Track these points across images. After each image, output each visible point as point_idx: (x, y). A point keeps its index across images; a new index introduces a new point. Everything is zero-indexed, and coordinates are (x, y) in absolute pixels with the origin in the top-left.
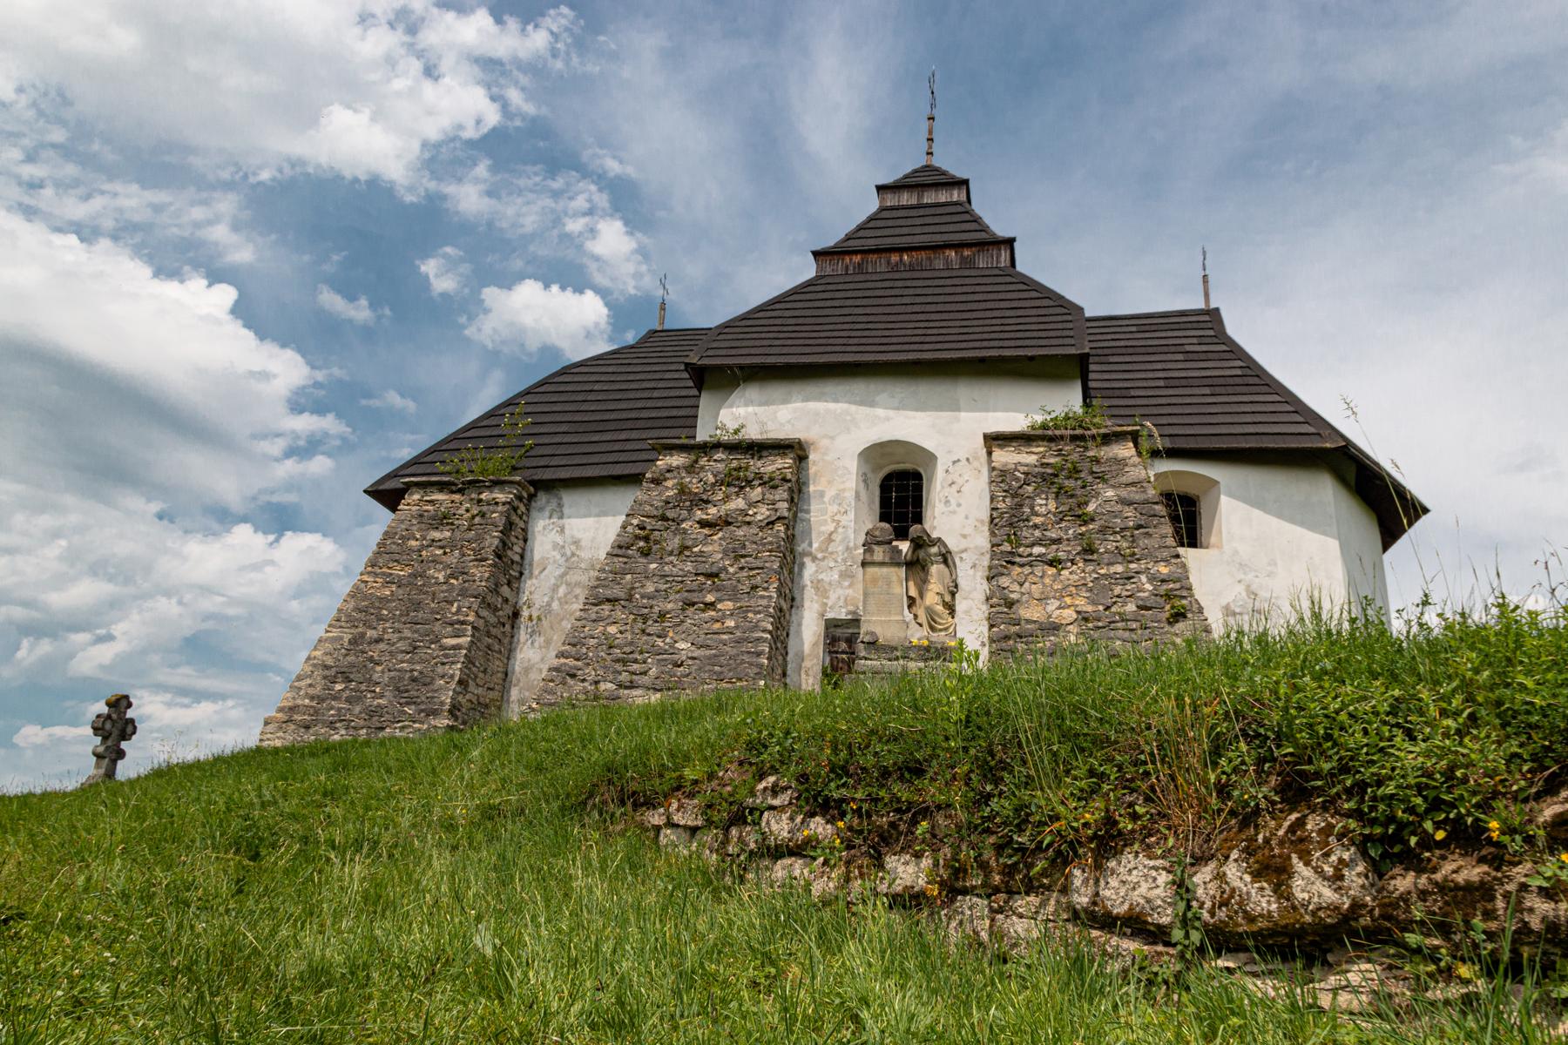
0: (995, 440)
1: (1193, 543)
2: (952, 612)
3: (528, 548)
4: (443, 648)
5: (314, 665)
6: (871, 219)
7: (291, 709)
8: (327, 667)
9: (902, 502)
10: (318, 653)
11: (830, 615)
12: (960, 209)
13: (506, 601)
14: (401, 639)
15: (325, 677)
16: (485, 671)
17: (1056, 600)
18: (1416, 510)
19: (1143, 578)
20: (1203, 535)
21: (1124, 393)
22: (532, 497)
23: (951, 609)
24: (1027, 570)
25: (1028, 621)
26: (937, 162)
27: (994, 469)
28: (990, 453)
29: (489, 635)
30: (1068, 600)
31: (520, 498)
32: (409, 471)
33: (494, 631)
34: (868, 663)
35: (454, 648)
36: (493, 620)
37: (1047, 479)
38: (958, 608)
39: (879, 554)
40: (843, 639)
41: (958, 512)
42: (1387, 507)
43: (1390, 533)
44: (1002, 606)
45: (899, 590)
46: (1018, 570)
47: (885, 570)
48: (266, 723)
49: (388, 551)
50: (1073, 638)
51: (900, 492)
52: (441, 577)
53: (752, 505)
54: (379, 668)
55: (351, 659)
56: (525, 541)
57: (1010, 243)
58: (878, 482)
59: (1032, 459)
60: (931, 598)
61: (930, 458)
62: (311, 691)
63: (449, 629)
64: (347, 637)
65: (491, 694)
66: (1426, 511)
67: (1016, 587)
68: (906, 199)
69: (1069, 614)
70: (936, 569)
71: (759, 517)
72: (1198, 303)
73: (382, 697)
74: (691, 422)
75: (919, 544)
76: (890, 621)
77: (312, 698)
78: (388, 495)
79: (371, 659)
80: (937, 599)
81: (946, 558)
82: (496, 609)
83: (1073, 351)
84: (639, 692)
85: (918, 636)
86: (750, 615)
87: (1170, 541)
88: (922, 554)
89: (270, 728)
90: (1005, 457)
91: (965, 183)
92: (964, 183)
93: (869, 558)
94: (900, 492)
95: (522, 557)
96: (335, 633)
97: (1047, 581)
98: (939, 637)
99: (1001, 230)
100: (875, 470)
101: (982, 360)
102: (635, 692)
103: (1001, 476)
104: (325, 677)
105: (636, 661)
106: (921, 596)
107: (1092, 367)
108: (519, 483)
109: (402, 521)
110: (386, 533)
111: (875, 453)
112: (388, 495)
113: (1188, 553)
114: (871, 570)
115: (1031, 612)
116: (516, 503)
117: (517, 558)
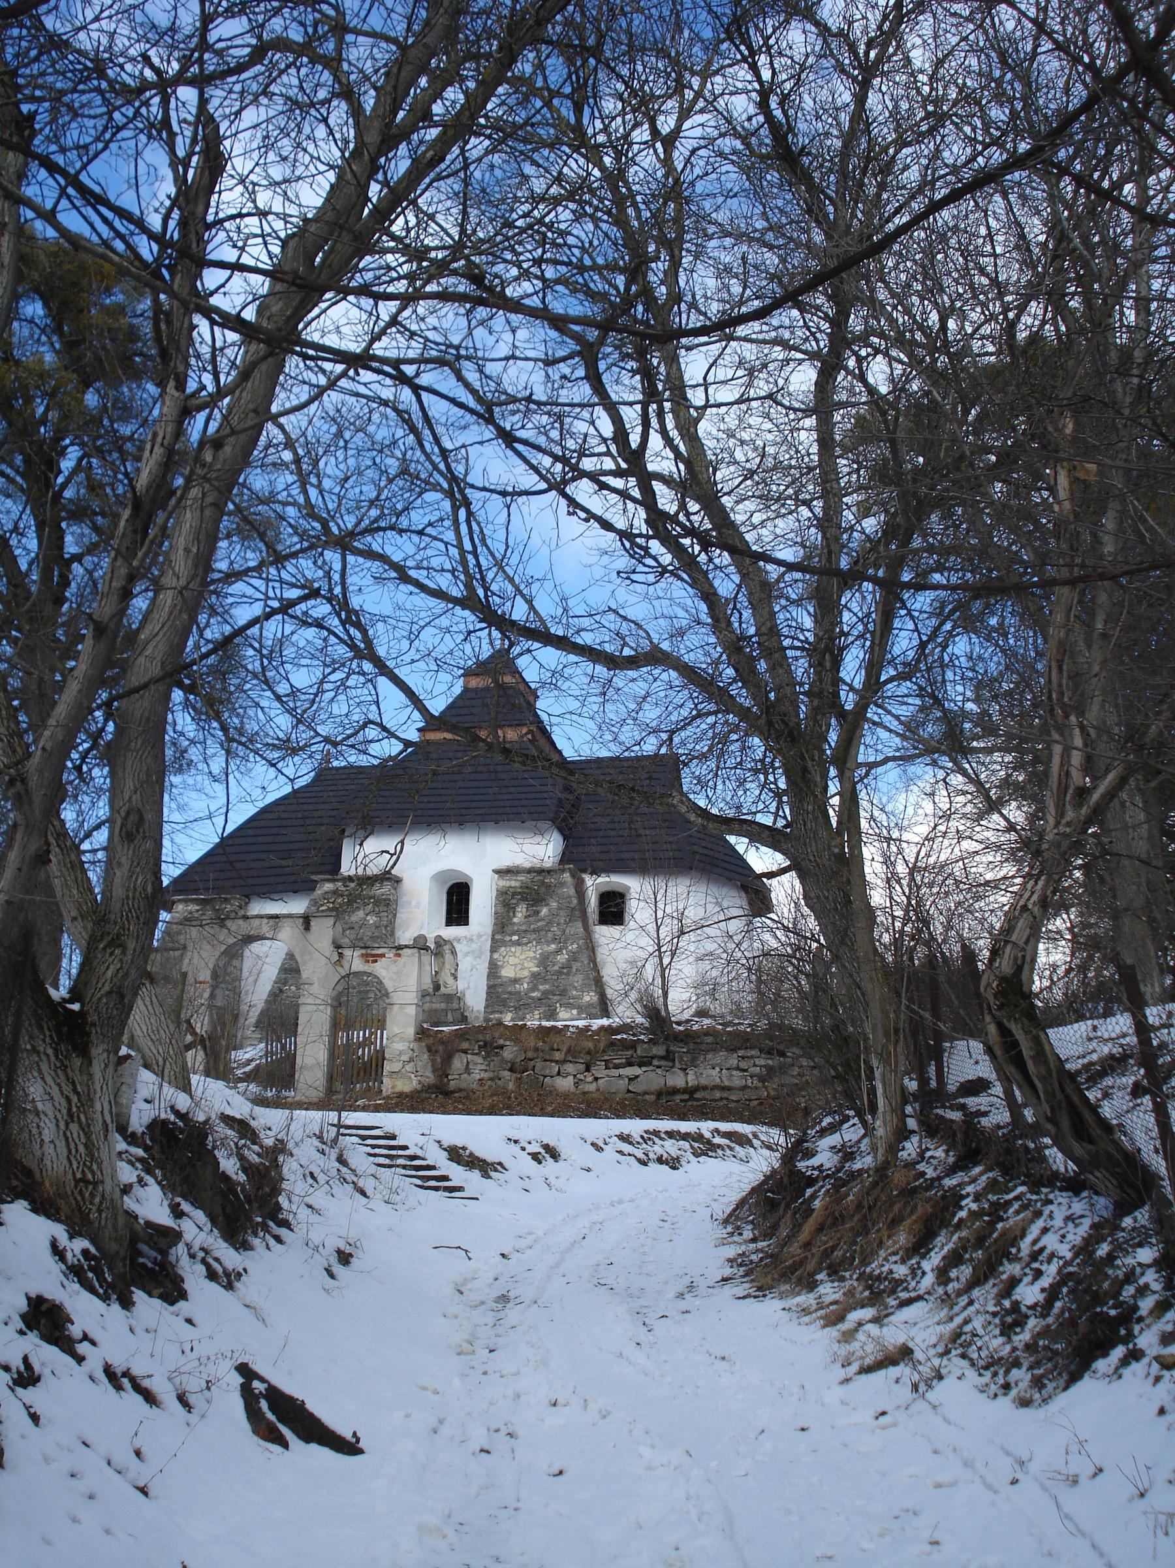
9: (459, 902)
44: (494, 969)
69: (526, 973)
70: (448, 957)
111: (439, 877)
115: (507, 972)
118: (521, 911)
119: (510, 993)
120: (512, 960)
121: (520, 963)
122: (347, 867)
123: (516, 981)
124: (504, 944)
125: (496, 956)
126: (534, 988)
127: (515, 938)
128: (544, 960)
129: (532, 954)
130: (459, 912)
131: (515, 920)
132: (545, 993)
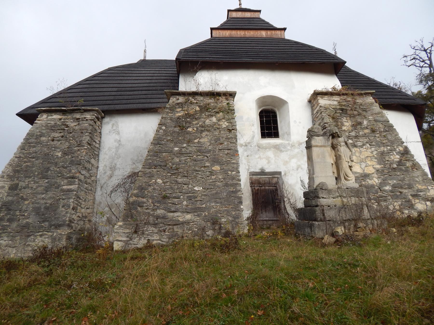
4: (63, 191)
9: (268, 122)
11: (252, 170)
13: (93, 165)
14: (39, 186)
16: (85, 201)
22: (103, 118)
31: (98, 118)
33: (89, 181)
35: (70, 190)
36: (87, 175)
47: (322, 149)
49: (29, 141)
50: (376, 180)
52: (59, 154)
53: (219, 120)
54: (26, 202)
55: (10, 198)
56: (100, 138)
59: (335, 103)
63: (66, 181)
64: (7, 188)
65: (88, 211)
71: (224, 126)
73: (28, 218)
78: (29, 116)
79: (22, 198)
82: (89, 170)
86: (230, 172)
90: (323, 102)
95: (100, 144)
100: (259, 107)
102: (176, 214)
105: (175, 198)
108: (97, 111)
109: (37, 128)
110: (28, 134)
116: (96, 120)
117: (97, 146)
129: (368, 153)
130: (269, 128)
132: (394, 186)
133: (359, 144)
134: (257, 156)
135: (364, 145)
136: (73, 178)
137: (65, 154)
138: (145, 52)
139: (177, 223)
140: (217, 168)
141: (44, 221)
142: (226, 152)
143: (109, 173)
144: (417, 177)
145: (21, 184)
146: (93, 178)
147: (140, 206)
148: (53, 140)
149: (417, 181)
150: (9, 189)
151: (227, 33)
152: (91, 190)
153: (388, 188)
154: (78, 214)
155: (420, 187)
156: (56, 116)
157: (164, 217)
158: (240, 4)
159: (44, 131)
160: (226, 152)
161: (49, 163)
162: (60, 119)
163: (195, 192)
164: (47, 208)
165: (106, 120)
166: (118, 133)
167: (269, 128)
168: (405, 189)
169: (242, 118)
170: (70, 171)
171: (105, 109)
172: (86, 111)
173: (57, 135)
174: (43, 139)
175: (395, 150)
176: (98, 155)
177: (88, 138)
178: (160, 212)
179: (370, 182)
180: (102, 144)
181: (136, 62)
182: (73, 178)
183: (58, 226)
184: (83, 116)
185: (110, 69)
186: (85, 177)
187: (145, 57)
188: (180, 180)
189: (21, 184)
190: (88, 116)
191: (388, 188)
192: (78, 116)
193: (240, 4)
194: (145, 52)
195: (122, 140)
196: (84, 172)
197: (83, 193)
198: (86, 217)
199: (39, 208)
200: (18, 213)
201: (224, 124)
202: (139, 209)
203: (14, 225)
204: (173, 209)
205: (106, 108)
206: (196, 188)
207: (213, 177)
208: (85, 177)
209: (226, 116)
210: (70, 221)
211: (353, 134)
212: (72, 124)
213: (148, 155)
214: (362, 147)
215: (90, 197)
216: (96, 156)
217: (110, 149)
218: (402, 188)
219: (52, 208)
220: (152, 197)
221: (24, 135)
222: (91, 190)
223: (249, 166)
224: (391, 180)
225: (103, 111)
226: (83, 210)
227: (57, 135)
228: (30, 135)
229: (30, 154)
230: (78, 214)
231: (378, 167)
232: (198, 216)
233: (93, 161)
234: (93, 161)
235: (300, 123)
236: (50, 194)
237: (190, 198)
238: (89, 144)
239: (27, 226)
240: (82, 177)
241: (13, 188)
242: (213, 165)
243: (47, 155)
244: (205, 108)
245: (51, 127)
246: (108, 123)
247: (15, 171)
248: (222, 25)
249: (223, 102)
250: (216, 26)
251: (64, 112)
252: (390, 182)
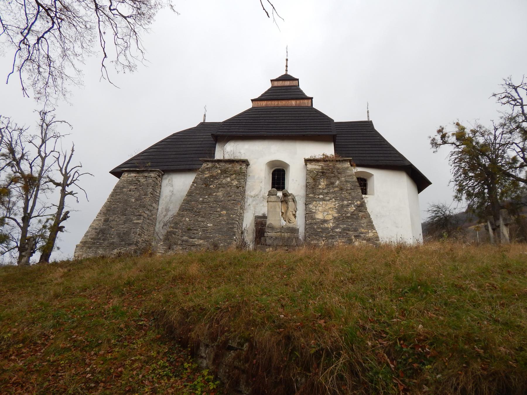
0: (307, 161)
1: (366, 194)
2: (295, 217)
3: (162, 191)
4: (134, 223)
5: (93, 229)
6: (269, 90)
7: (85, 242)
8: (96, 229)
10: (94, 225)
11: (257, 215)
12: (296, 88)
13: (154, 208)
15: (96, 232)
16: (147, 231)
17: (326, 211)
18: (429, 183)
19: (353, 206)
20: (368, 190)
21: (346, 146)
22: (163, 175)
23: (295, 216)
24: (318, 203)
25: (318, 219)
26: (289, 73)
27: (307, 170)
28: (306, 165)
29: (148, 219)
30: (330, 212)
31: (159, 176)
32: (125, 166)
34: (269, 234)
36: (150, 214)
37: (323, 173)
38: (297, 215)
39: (273, 198)
40: (261, 224)
41: (295, 183)
42: (421, 182)
43: (420, 190)
45: (279, 210)
46: (315, 202)
47: (274, 203)
48: (77, 247)
50: (331, 224)
51: (278, 175)
52: (133, 200)
53: (232, 180)
54: (113, 230)
55: (104, 227)
57: (312, 98)
58: (271, 172)
60: (290, 214)
61: (287, 165)
62: (92, 237)
64: (103, 220)
66: (429, 183)
67: (314, 208)
68: (280, 83)
69: (330, 217)
70: (291, 203)
71: (234, 184)
72: (367, 120)
74: (212, 153)
75: (285, 195)
76: (276, 220)
77: (92, 239)
78: (117, 173)
79: (111, 227)
80: (291, 213)
81: (294, 201)
82: (151, 211)
83: (330, 133)
84: (196, 240)
85: (284, 223)
87: (360, 194)
88: (286, 199)
89: (78, 248)
90: (310, 166)
91: (298, 80)
92: (298, 80)
93: (269, 200)
94: (278, 175)
95: (160, 193)
96: (99, 218)
97: (324, 206)
98: (291, 225)
99: (308, 95)
100: (271, 168)
101: (304, 136)
102: (194, 240)
103: (309, 172)
104: (96, 232)
105: (195, 230)
106: (286, 212)
107: (337, 138)
110: (116, 186)
112: (117, 173)
113: (364, 196)
114: (270, 203)
115: (320, 216)
116: (158, 177)
117: (158, 194)
118: (323, 183)
119: (322, 228)
120: (320, 209)
121: (326, 211)
122: (218, 155)
123: (325, 221)
124: (313, 199)
125: (311, 206)
126: (337, 227)
127: (321, 196)
128: (341, 209)
129: (332, 206)
130: (278, 184)
131: (320, 187)
132: (344, 229)
133: (328, 198)
134: (261, 205)
135: (330, 199)
136: (140, 215)
137: (137, 200)
138: (205, 116)
139: (194, 245)
140: (224, 212)
141: (122, 241)
142: (232, 202)
143: (164, 213)
144: (363, 224)
145: (111, 218)
146: (154, 216)
147: (175, 234)
148: (130, 191)
149: (362, 226)
150: (104, 221)
151: (264, 104)
152: (152, 224)
153: (338, 230)
154: (142, 239)
155: (363, 230)
156: (133, 175)
157: (187, 241)
158: (287, 71)
159: (125, 185)
160: (232, 202)
161: (127, 205)
162: (135, 177)
163: (207, 227)
164: (124, 234)
165: (165, 176)
166: (172, 186)
167: (278, 184)
168: (352, 231)
169: (254, 177)
170: (139, 211)
171: (164, 169)
172: (151, 171)
173: (133, 187)
174: (124, 190)
175: (354, 204)
176: (158, 201)
177: (151, 190)
178: (185, 238)
179: (326, 225)
180: (162, 193)
181: (195, 125)
182: (140, 215)
183: (130, 244)
184: (149, 175)
185: (174, 135)
186: (148, 215)
187: (204, 120)
188: (199, 219)
189: (111, 218)
190: (152, 175)
191: (338, 230)
192: (146, 174)
193: (287, 71)
194: (205, 116)
195: (174, 190)
196: (147, 212)
197: (146, 226)
198: (148, 241)
199: (120, 233)
200: (108, 236)
201: (235, 183)
202: (173, 235)
203: (106, 242)
204: (193, 237)
205: (165, 168)
206: (208, 225)
207: (220, 218)
208: (148, 215)
209: (238, 177)
210: (137, 242)
211: (325, 191)
212: (142, 180)
213: (183, 203)
214: (329, 200)
215: (151, 229)
216: (157, 202)
217: (166, 197)
218: (349, 230)
219: (127, 234)
220: (182, 229)
221: (113, 187)
222: (152, 224)
223: (255, 211)
224: (342, 225)
225: (163, 171)
226: (146, 237)
227: (133, 187)
228: (117, 187)
229: (116, 199)
230: (142, 239)
231: (336, 215)
232: (207, 241)
233: (154, 205)
234: (154, 205)
235: (296, 181)
236: (126, 225)
237: (204, 231)
238: (152, 194)
239: (113, 243)
240: (146, 216)
241: (106, 221)
242: (221, 211)
243: (126, 200)
244: (224, 172)
245: (130, 182)
246: (166, 178)
247: (108, 210)
248: (262, 95)
249: (237, 167)
250: (257, 97)
251: (138, 172)
252: (341, 226)
